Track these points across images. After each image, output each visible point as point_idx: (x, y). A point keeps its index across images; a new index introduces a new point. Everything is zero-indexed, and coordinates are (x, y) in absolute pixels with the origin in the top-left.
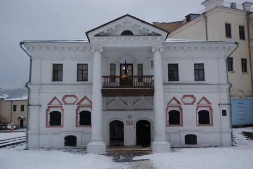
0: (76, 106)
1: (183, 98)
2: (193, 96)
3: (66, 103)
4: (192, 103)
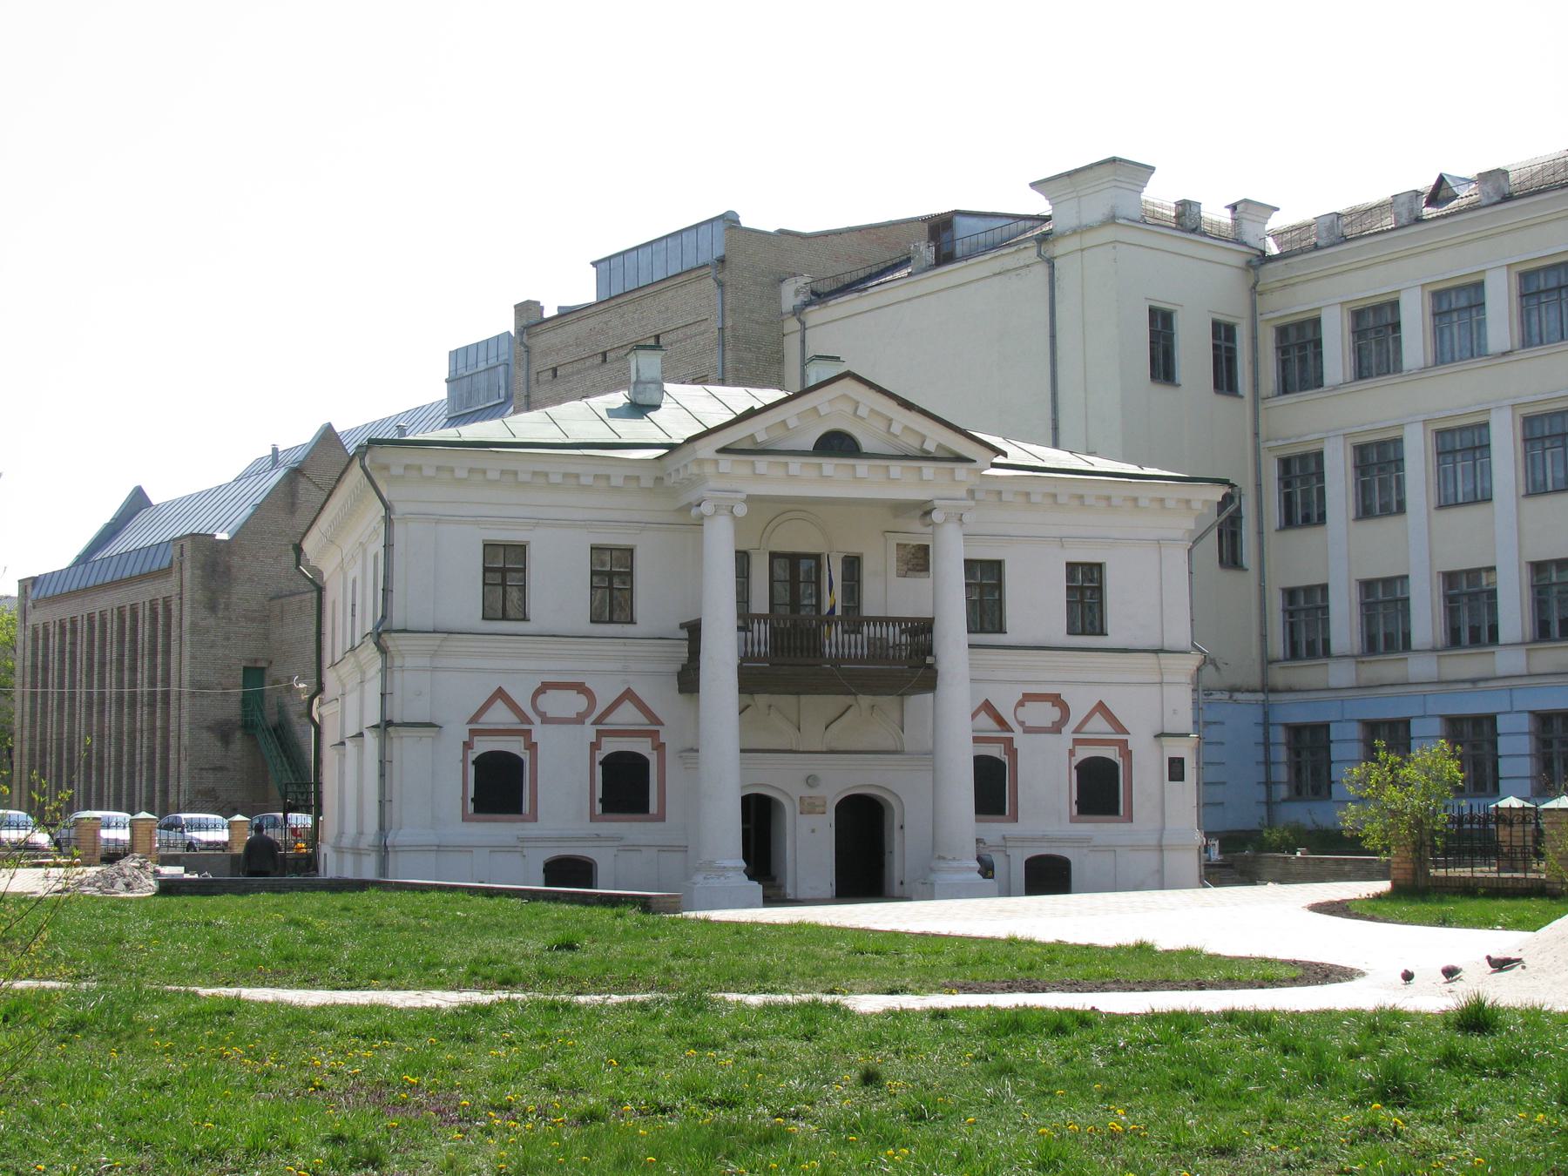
0: (589, 732)
1: (1021, 704)
2: (1059, 695)
3: (546, 720)
4: (1056, 728)
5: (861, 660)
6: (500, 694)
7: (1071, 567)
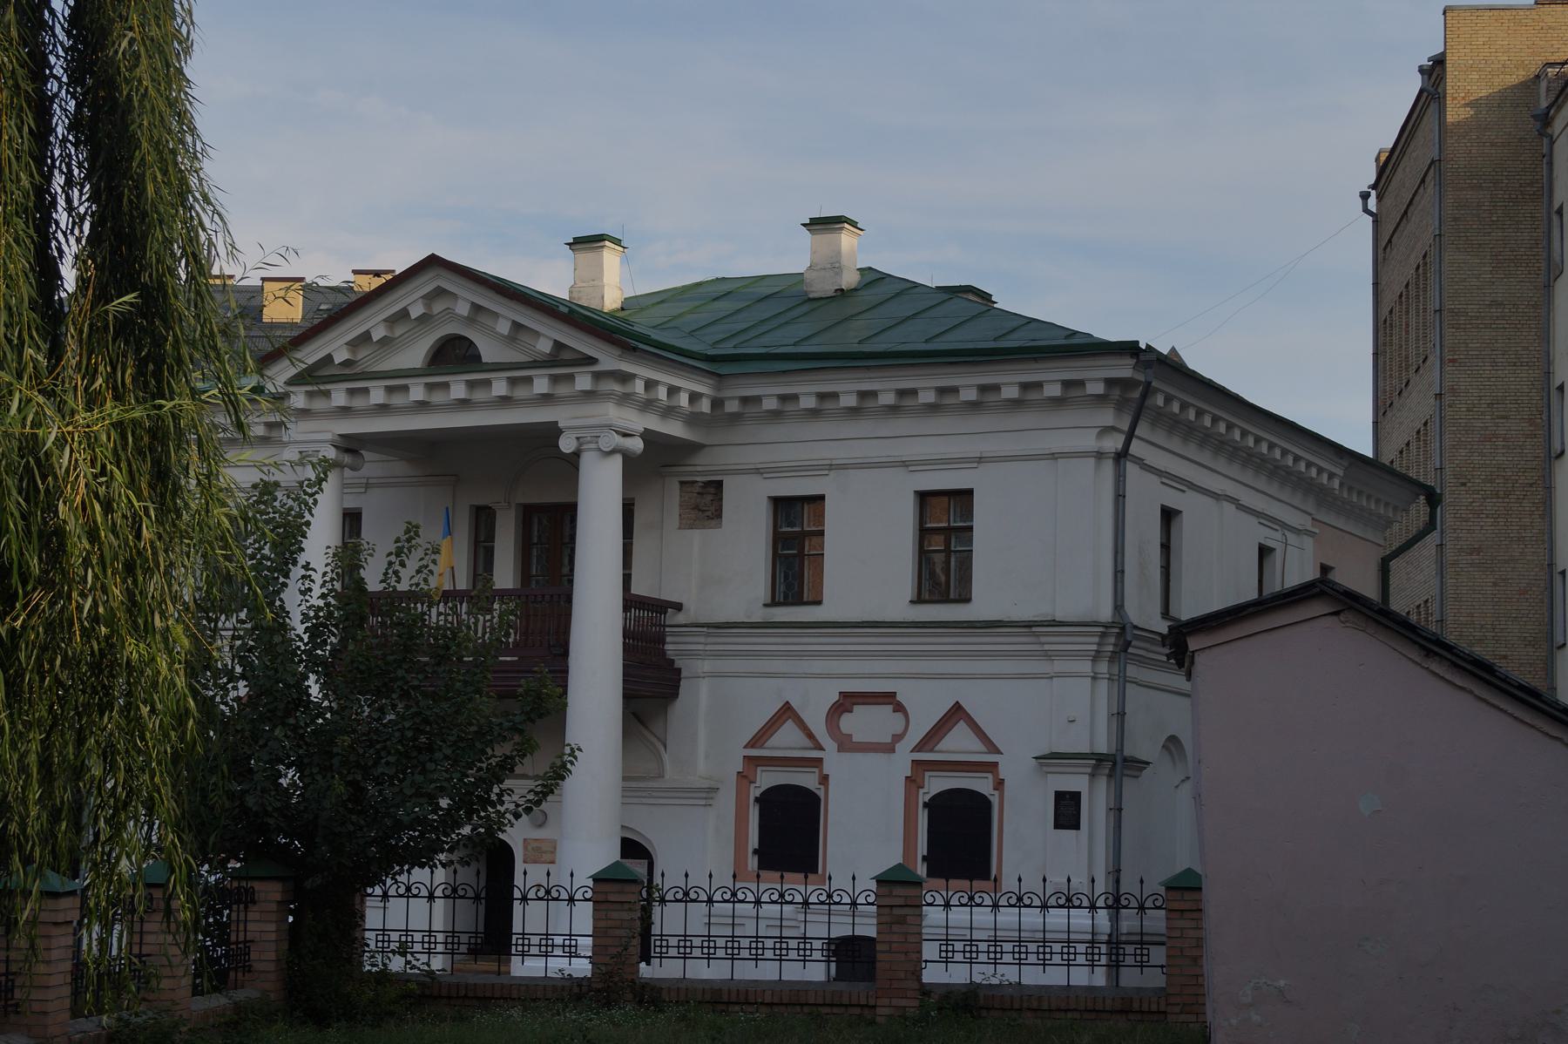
2: (893, 695)
7: (924, 498)
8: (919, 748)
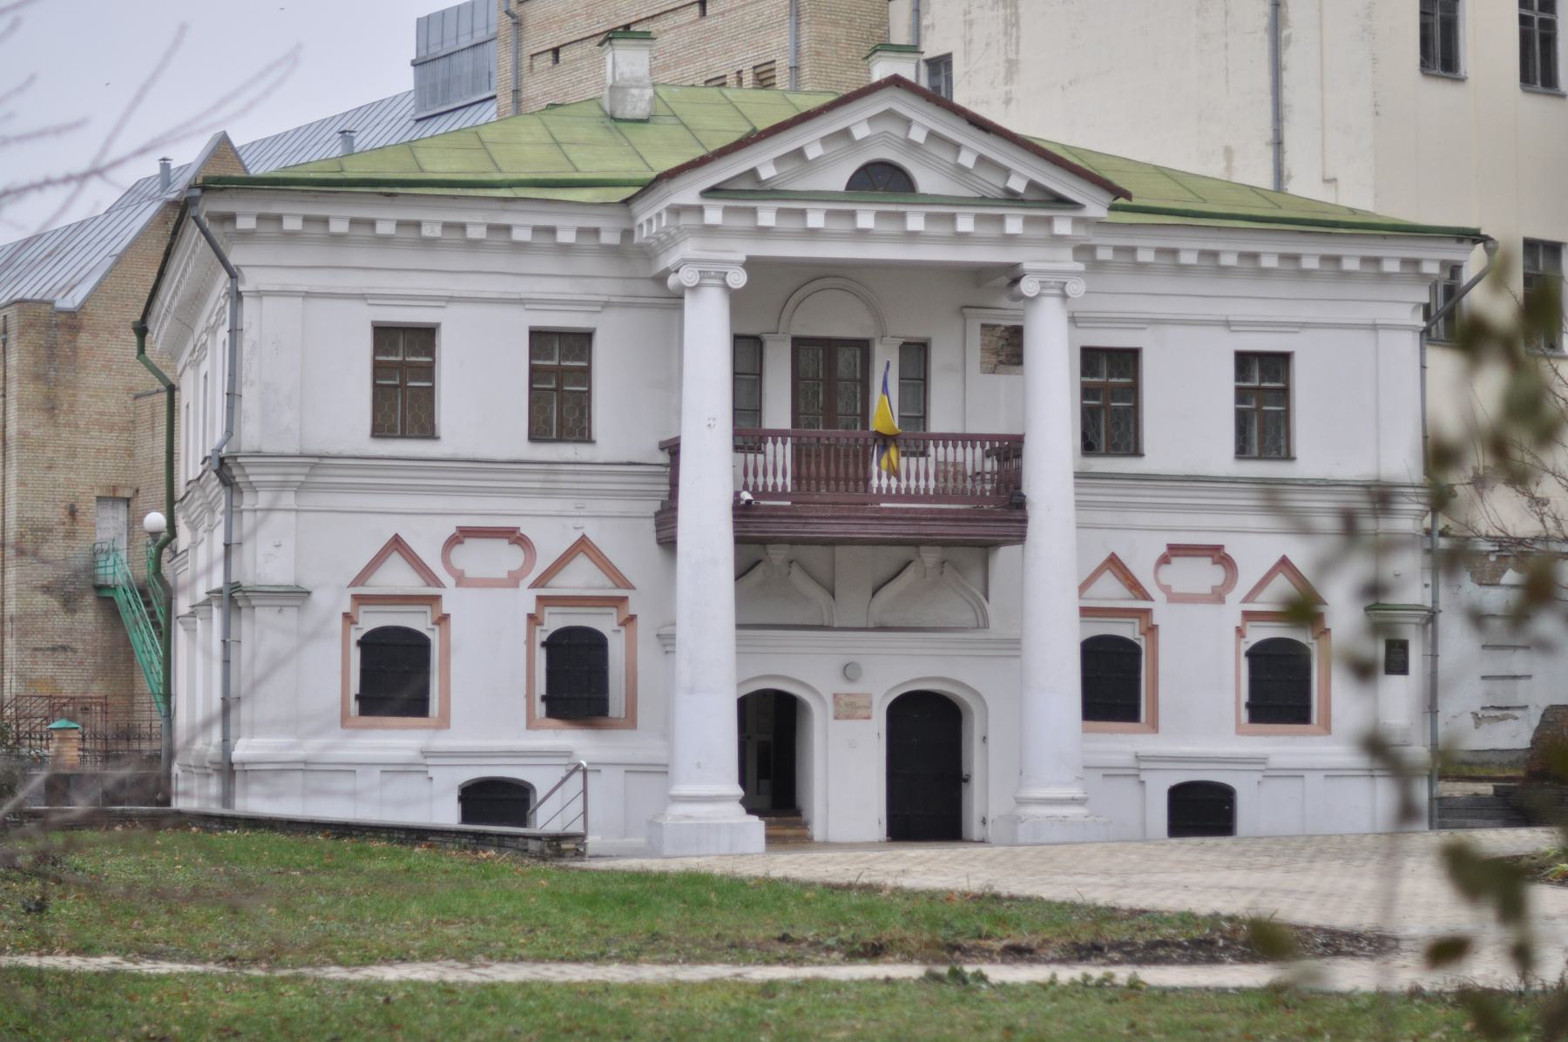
0: (526, 600)
1: (1164, 560)
2: (1219, 548)
3: (461, 580)
4: (1218, 596)
5: (926, 498)
6: (397, 544)
7: (1244, 361)
8: (1247, 600)
